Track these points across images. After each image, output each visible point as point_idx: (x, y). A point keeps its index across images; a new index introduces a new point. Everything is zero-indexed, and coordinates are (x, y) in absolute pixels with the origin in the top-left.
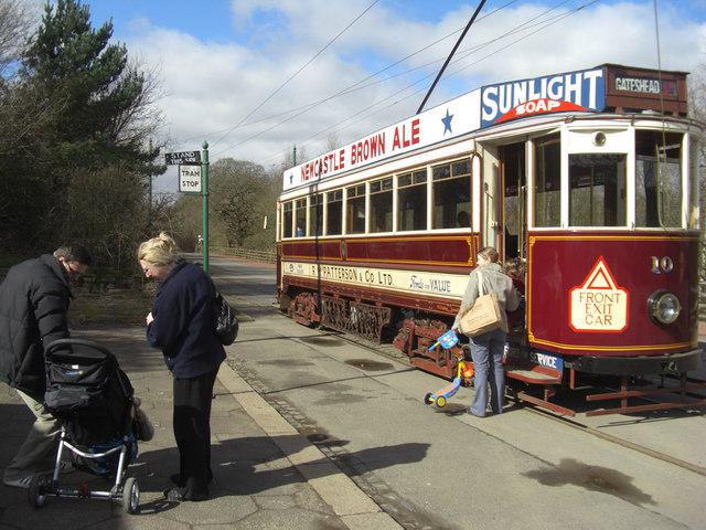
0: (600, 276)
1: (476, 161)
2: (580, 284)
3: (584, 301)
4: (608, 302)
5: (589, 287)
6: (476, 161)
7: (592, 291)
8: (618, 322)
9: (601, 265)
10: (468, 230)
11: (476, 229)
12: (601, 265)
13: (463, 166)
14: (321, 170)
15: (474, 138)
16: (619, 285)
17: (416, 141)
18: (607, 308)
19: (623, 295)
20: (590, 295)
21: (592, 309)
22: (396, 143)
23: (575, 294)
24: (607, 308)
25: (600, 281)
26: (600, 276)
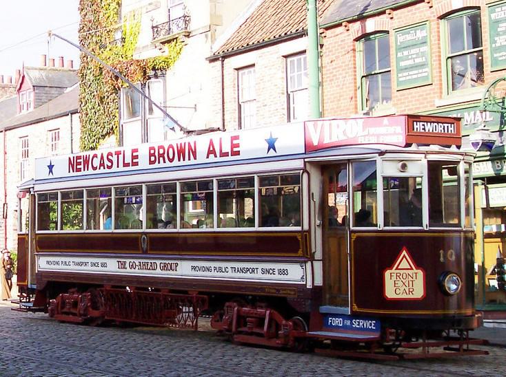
0: (404, 260)
1: (305, 176)
2: (391, 267)
3: (394, 278)
5: (397, 269)
6: (305, 176)
7: (402, 272)
8: (418, 292)
9: (404, 253)
10: (299, 228)
11: (306, 227)
12: (404, 253)
13: (294, 179)
15: (304, 159)
16: (418, 267)
18: (411, 283)
19: (420, 273)
20: (398, 275)
21: (400, 284)
24: (411, 283)
25: (404, 264)
26: (404, 260)
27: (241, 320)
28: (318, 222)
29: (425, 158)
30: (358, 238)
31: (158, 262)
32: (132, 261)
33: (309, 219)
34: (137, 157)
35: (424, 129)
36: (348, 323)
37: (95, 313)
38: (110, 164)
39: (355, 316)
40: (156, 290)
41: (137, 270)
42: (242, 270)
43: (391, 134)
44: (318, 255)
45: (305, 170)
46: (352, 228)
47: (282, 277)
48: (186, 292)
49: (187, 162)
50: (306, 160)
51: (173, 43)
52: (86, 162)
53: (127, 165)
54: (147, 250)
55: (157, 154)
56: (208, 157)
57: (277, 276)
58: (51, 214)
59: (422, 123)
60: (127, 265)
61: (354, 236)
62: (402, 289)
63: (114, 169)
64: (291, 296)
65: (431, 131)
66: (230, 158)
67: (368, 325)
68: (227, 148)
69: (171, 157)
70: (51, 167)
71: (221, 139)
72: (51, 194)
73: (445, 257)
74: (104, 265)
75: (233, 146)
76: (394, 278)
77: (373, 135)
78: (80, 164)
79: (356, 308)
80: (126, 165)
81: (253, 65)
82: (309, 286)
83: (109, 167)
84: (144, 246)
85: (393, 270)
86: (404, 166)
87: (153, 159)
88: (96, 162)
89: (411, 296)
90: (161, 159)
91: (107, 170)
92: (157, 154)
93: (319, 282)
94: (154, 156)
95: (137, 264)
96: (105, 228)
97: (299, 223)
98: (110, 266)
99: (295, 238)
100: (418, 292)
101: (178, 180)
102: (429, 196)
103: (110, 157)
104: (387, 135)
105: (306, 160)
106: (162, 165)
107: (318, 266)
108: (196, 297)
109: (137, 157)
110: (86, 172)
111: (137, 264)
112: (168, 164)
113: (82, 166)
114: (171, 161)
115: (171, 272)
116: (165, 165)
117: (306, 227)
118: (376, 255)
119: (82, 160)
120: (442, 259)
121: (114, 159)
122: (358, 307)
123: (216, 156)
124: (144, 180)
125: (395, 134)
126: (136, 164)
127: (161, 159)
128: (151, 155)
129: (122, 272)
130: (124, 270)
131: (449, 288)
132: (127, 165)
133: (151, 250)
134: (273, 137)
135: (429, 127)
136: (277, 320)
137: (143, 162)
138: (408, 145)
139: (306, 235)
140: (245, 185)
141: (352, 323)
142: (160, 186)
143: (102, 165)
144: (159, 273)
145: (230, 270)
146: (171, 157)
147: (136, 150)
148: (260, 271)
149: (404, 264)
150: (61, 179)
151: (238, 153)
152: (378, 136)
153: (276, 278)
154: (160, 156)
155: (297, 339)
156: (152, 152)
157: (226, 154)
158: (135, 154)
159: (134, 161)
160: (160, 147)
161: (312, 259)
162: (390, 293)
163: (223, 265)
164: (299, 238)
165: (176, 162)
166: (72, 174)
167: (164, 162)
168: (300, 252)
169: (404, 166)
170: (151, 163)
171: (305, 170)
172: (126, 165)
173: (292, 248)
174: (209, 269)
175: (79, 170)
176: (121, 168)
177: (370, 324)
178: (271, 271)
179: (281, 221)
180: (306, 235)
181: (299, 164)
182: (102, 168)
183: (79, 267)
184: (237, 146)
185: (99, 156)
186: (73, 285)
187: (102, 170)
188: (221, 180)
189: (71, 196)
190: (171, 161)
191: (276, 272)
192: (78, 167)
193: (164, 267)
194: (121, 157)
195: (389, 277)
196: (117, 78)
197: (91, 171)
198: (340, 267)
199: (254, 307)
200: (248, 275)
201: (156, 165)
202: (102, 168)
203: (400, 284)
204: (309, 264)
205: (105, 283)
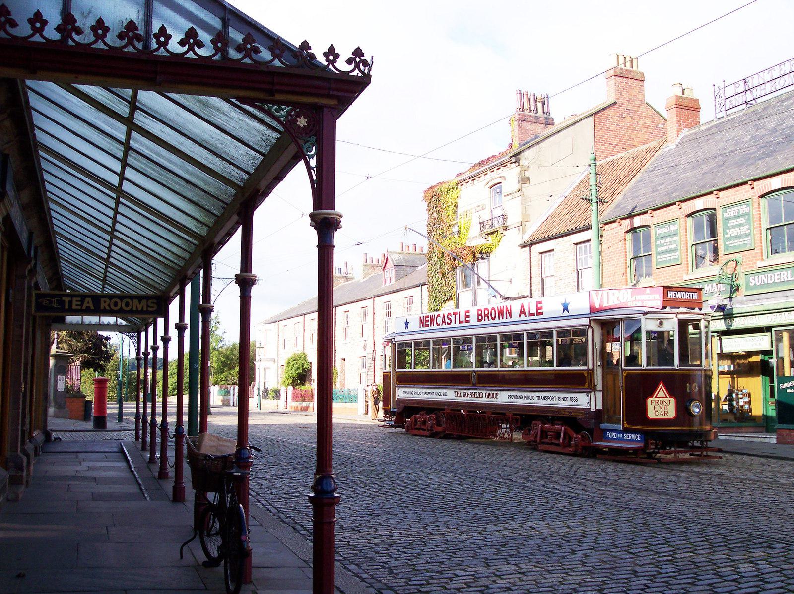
1: (590, 330)
2: (651, 396)
3: (654, 404)
4: (666, 404)
5: (656, 397)
6: (590, 330)
7: (659, 399)
8: (671, 414)
9: (661, 385)
12: (661, 385)
13: (582, 332)
18: (666, 407)
19: (673, 400)
21: (658, 408)
23: (649, 400)
24: (666, 407)
25: (661, 394)
27: (544, 433)
28: (599, 363)
29: (676, 317)
30: (628, 375)
31: (484, 392)
32: (465, 391)
33: (593, 361)
34: (469, 316)
35: (675, 296)
36: (621, 436)
37: (439, 429)
38: (449, 322)
39: (626, 431)
40: (483, 412)
41: (469, 398)
42: (544, 398)
43: (651, 300)
44: (599, 387)
45: (590, 326)
46: (623, 368)
47: (573, 403)
48: (504, 414)
49: (505, 320)
50: (591, 319)
51: (495, 234)
52: (432, 320)
53: (462, 322)
54: (476, 384)
55: (483, 314)
56: (520, 317)
57: (569, 402)
58: (407, 358)
59: (674, 292)
60: (462, 395)
61: (625, 374)
62: (660, 412)
63: (453, 325)
64: (580, 417)
65: (680, 298)
66: (536, 317)
67: (635, 437)
68: (533, 310)
69: (493, 316)
70: (407, 324)
71: (529, 304)
72: (407, 343)
73: (690, 388)
74: (445, 394)
75: (538, 308)
76: (654, 404)
77: (639, 300)
78: (428, 321)
79: (626, 425)
80: (461, 322)
81: (552, 250)
82: (593, 409)
83: (449, 324)
84: (474, 381)
85: (653, 398)
86: (661, 323)
87: (480, 318)
88: (440, 320)
89: (666, 417)
90: (486, 318)
91: (447, 326)
92: (483, 314)
93: (600, 406)
94: (481, 316)
95: (469, 393)
96: (445, 368)
97: (585, 364)
98: (450, 395)
99: (583, 375)
100: (671, 414)
101: (498, 333)
102: (679, 344)
103: (449, 317)
104: (649, 300)
105: (591, 319)
106: (487, 322)
107: (599, 395)
108: (512, 418)
109: (469, 316)
110: (432, 328)
111: (469, 393)
112: (491, 321)
113: (429, 323)
114: (493, 319)
115: (493, 399)
116: (489, 322)
117: (590, 367)
118: (641, 387)
119: (429, 319)
120: (688, 390)
121: (452, 318)
122: (628, 424)
123: (525, 316)
124: (474, 333)
125: (655, 300)
126: (468, 321)
127: (486, 318)
128: (479, 315)
129: (458, 399)
130: (459, 398)
131: (694, 411)
132: (462, 322)
133: (479, 383)
134: (567, 302)
135: (679, 295)
136: (570, 434)
137: (473, 320)
138: (664, 308)
139: (591, 372)
140: (547, 337)
141: (623, 436)
142: (485, 337)
143: (444, 322)
144: (484, 400)
145: (536, 398)
146: (493, 316)
147: (468, 312)
148: (557, 398)
149: (661, 394)
150: (414, 332)
151: (541, 314)
152: (642, 301)
153: (569, 404)
155: (584, 448)
156: (480, 313)
157: (533, 315)
158: (467, 314)
159: (467, 319)
160: (485, 309)
161: (595, 390)
162: (651, 414)
163: (531, 394)
164: (586, 374)
165: (497, 320)
166: (422, 329)
167: (489, 320)
168: (586, 385)
169: (661, 323)
170: (479, 320)
171: (590, 326)
172: (461, 322)
173: (581, 382)
174: (520, 397)
175: (427, 326)
176: (458, 325)
177: (636, 437)
178: (565, 399)
179: (572, 363)
180: (590, 373)
181: (585, 321)
182: (444, 324)
183: (427, 396)
184: (541, 308)
185: (442, 316)
186: (422, 409)
187: (444, 326)
188: (529, 333)
189: (422, 344)
190: (493, 319)
191: (569, 400)
192: (427, 323)
193: (489, 396)
194: (457, 316)
195: (651, 403)
196: (454, 259)
197: (436, 327)
198: (615, 396)
199: (553, 424)
200: (549, 401)
201: (483, 322)
202: (444, 324)
203: (658, 408)
204: (592, 394)
205: (446, 407)
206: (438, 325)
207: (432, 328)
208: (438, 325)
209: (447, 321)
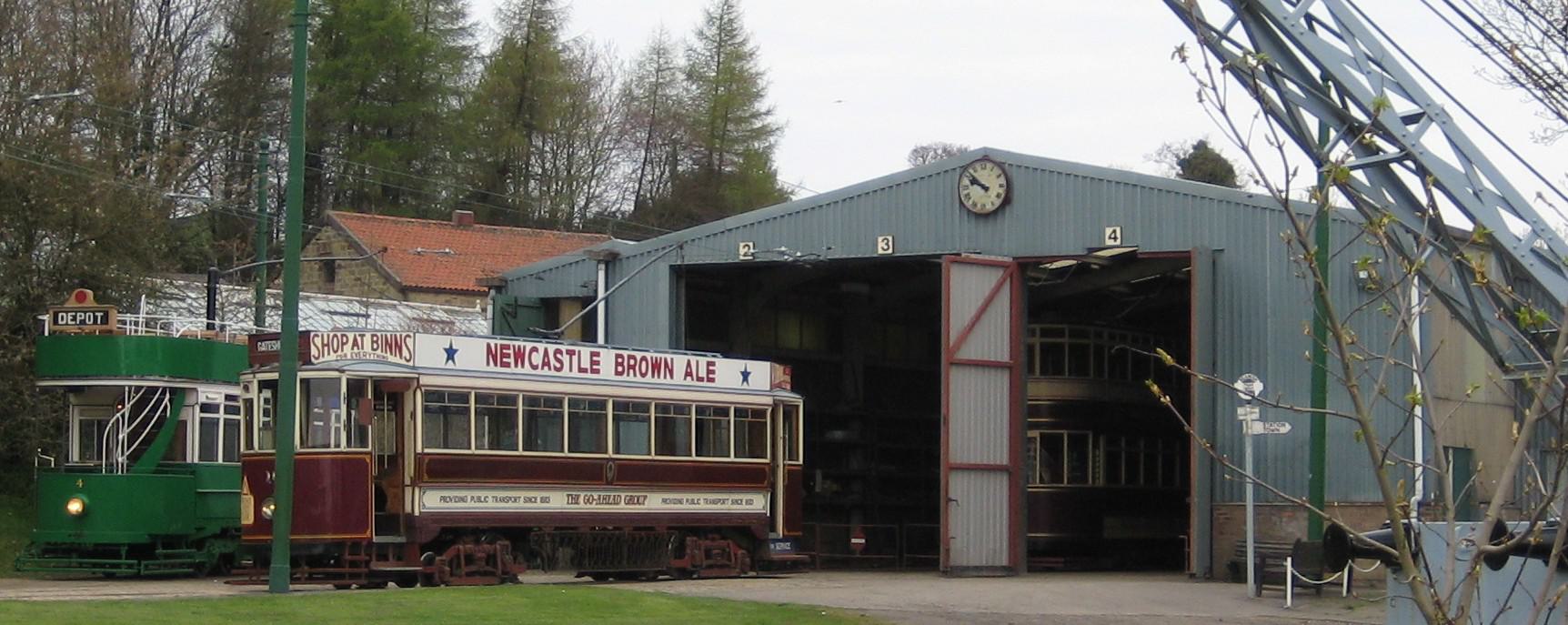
14: (546, 364)
17: (712, 380)
22: (689, 374)
49: (662, 380)
53: (585, 371)
80: (581, 370)
91: (553, 373)
106: (631, 378)
113: (512, 360)
114: (643, 375)
121: (566, 359)
128: (617, 364)
132: (585, 371)
154: (630, 367)
165: (649, 378)
166: (492, 368)
170: (617, 373)
175: (508, 365)
176: (575, 373)
190: (643, 375)
194: (575, 358)
197: (527, 369)
201: (624, 378)
206: (535, 367)
207: (519, 370)
208: (535, 367)
209: (553, 361)
